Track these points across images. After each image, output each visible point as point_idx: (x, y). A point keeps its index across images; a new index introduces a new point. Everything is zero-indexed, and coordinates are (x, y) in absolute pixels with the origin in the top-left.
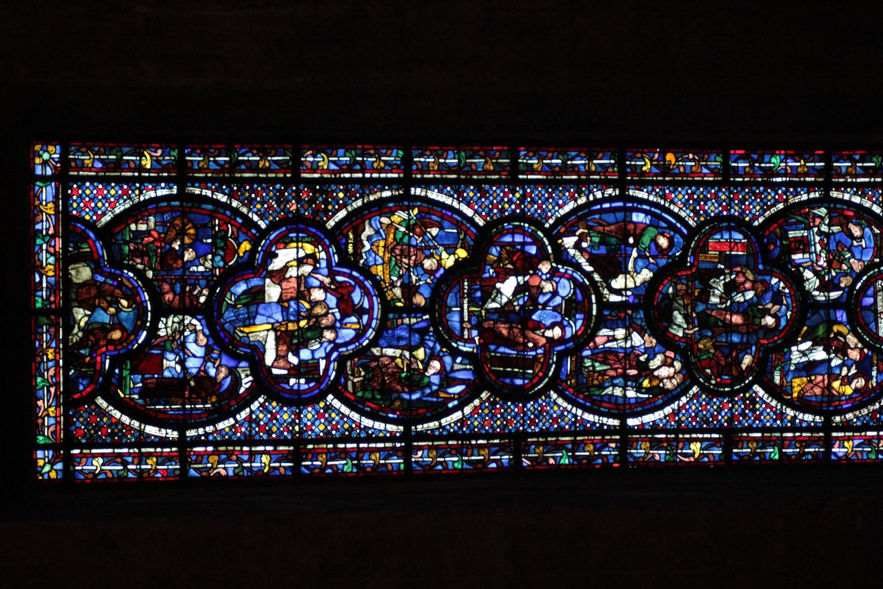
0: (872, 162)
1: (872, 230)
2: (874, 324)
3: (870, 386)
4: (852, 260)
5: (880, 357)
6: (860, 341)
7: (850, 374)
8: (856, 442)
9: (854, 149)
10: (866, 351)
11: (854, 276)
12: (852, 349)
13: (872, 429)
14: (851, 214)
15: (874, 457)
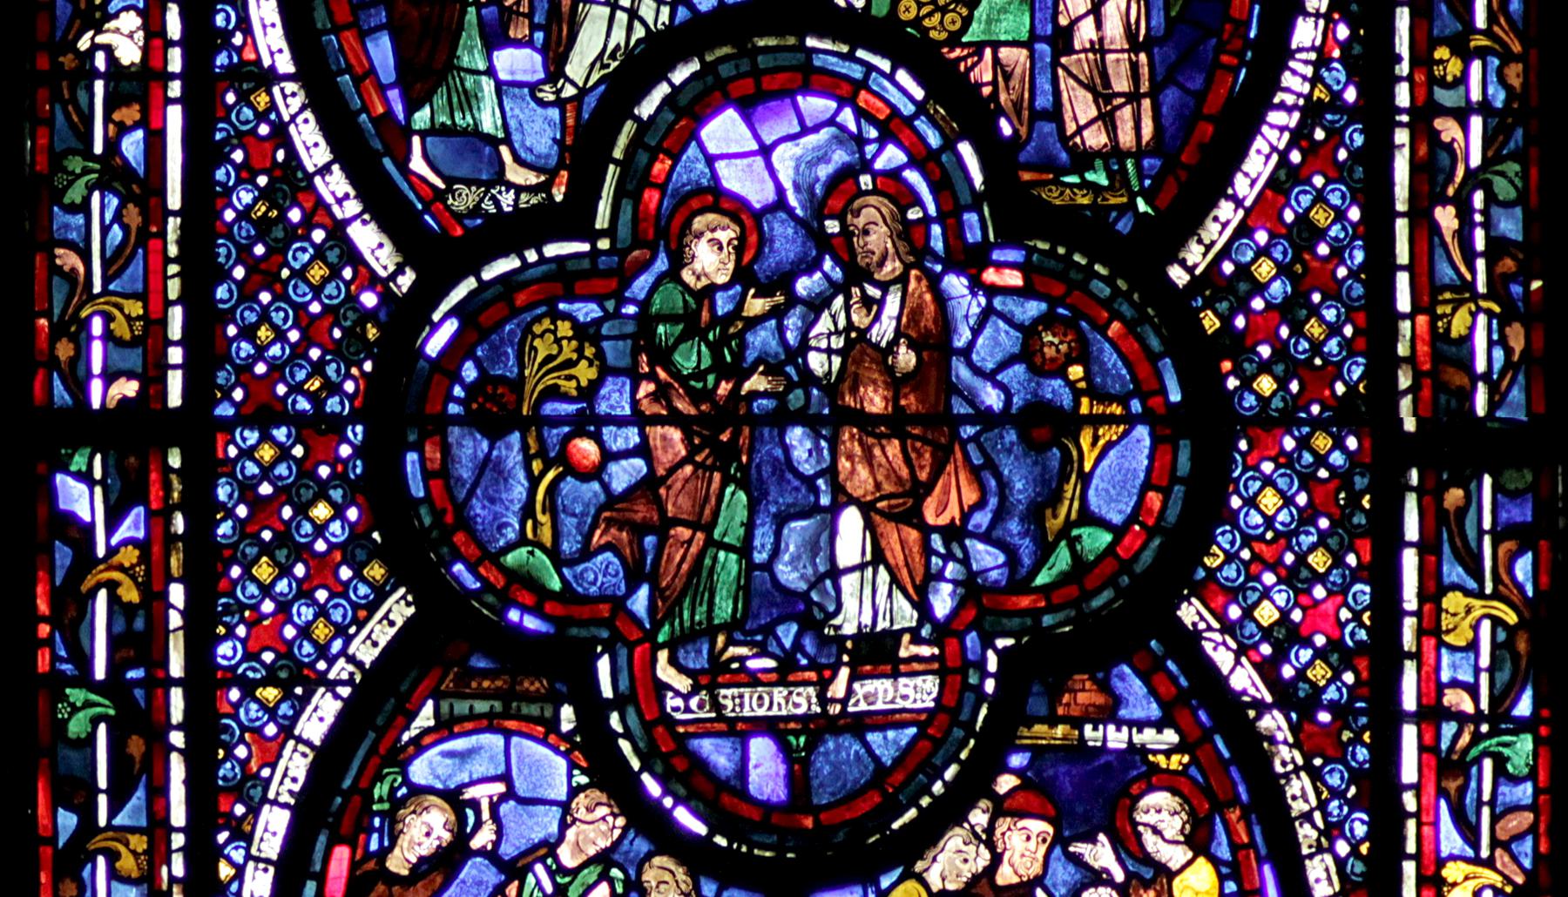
0: (91, 739)
1: (419, 746)
2: (873, 737)
3: (1175, 762)
4: (567, 856)
5: (1037, 705)
6: (960, 818)
7: (1119, 876)
8: (1451, 840)
9: (33, 837)
10: (1006, 783)
11: (642, 846)
12: (997, 859)
13: (1388, 752)
14: (342, 854)
15: (1526, 743)
